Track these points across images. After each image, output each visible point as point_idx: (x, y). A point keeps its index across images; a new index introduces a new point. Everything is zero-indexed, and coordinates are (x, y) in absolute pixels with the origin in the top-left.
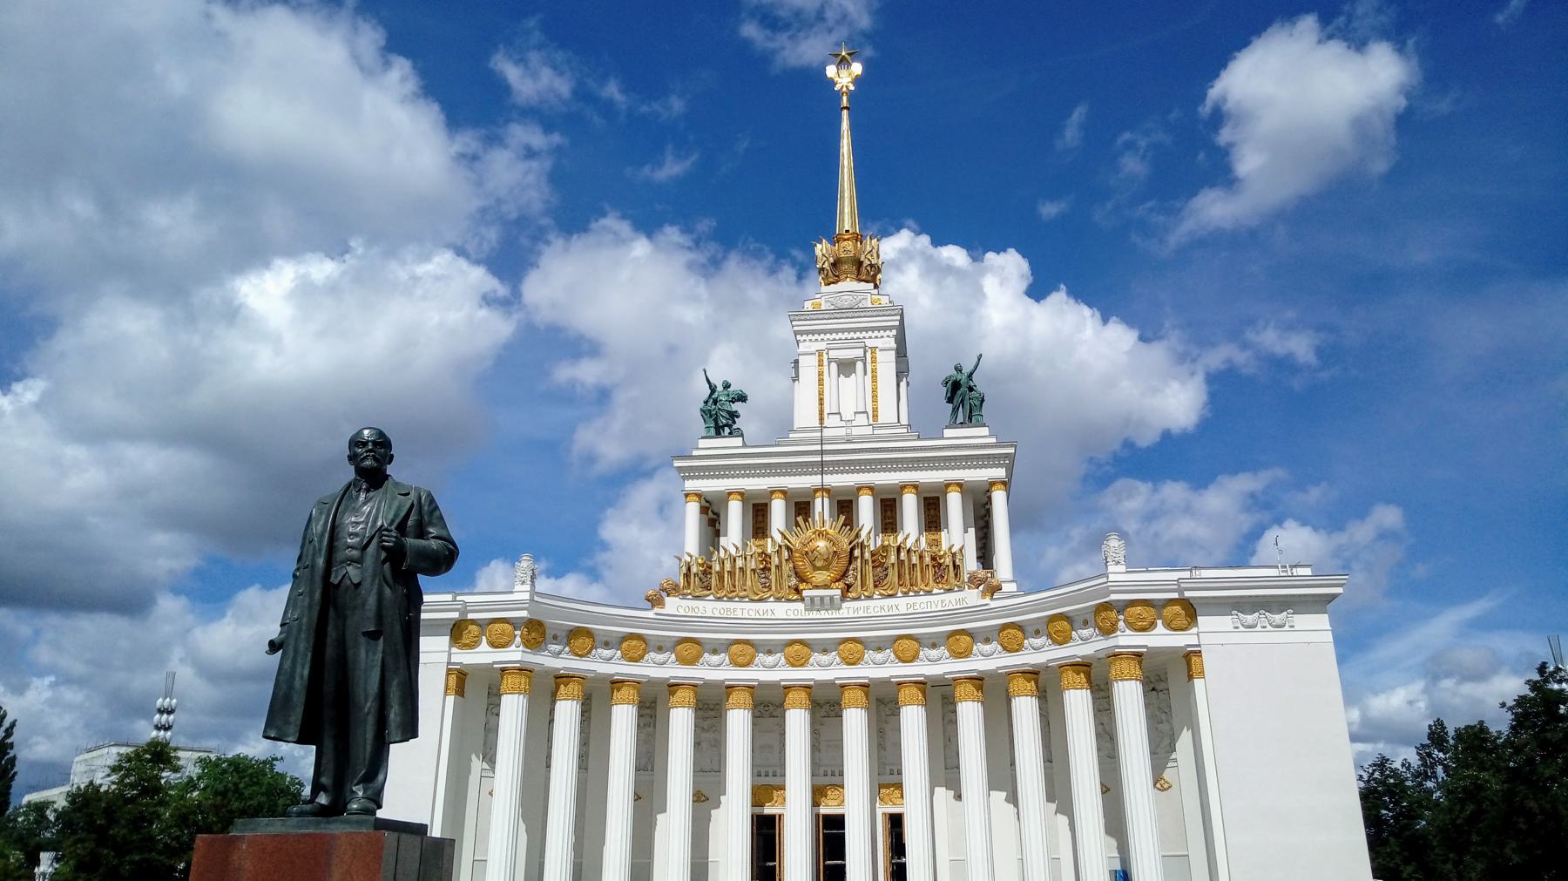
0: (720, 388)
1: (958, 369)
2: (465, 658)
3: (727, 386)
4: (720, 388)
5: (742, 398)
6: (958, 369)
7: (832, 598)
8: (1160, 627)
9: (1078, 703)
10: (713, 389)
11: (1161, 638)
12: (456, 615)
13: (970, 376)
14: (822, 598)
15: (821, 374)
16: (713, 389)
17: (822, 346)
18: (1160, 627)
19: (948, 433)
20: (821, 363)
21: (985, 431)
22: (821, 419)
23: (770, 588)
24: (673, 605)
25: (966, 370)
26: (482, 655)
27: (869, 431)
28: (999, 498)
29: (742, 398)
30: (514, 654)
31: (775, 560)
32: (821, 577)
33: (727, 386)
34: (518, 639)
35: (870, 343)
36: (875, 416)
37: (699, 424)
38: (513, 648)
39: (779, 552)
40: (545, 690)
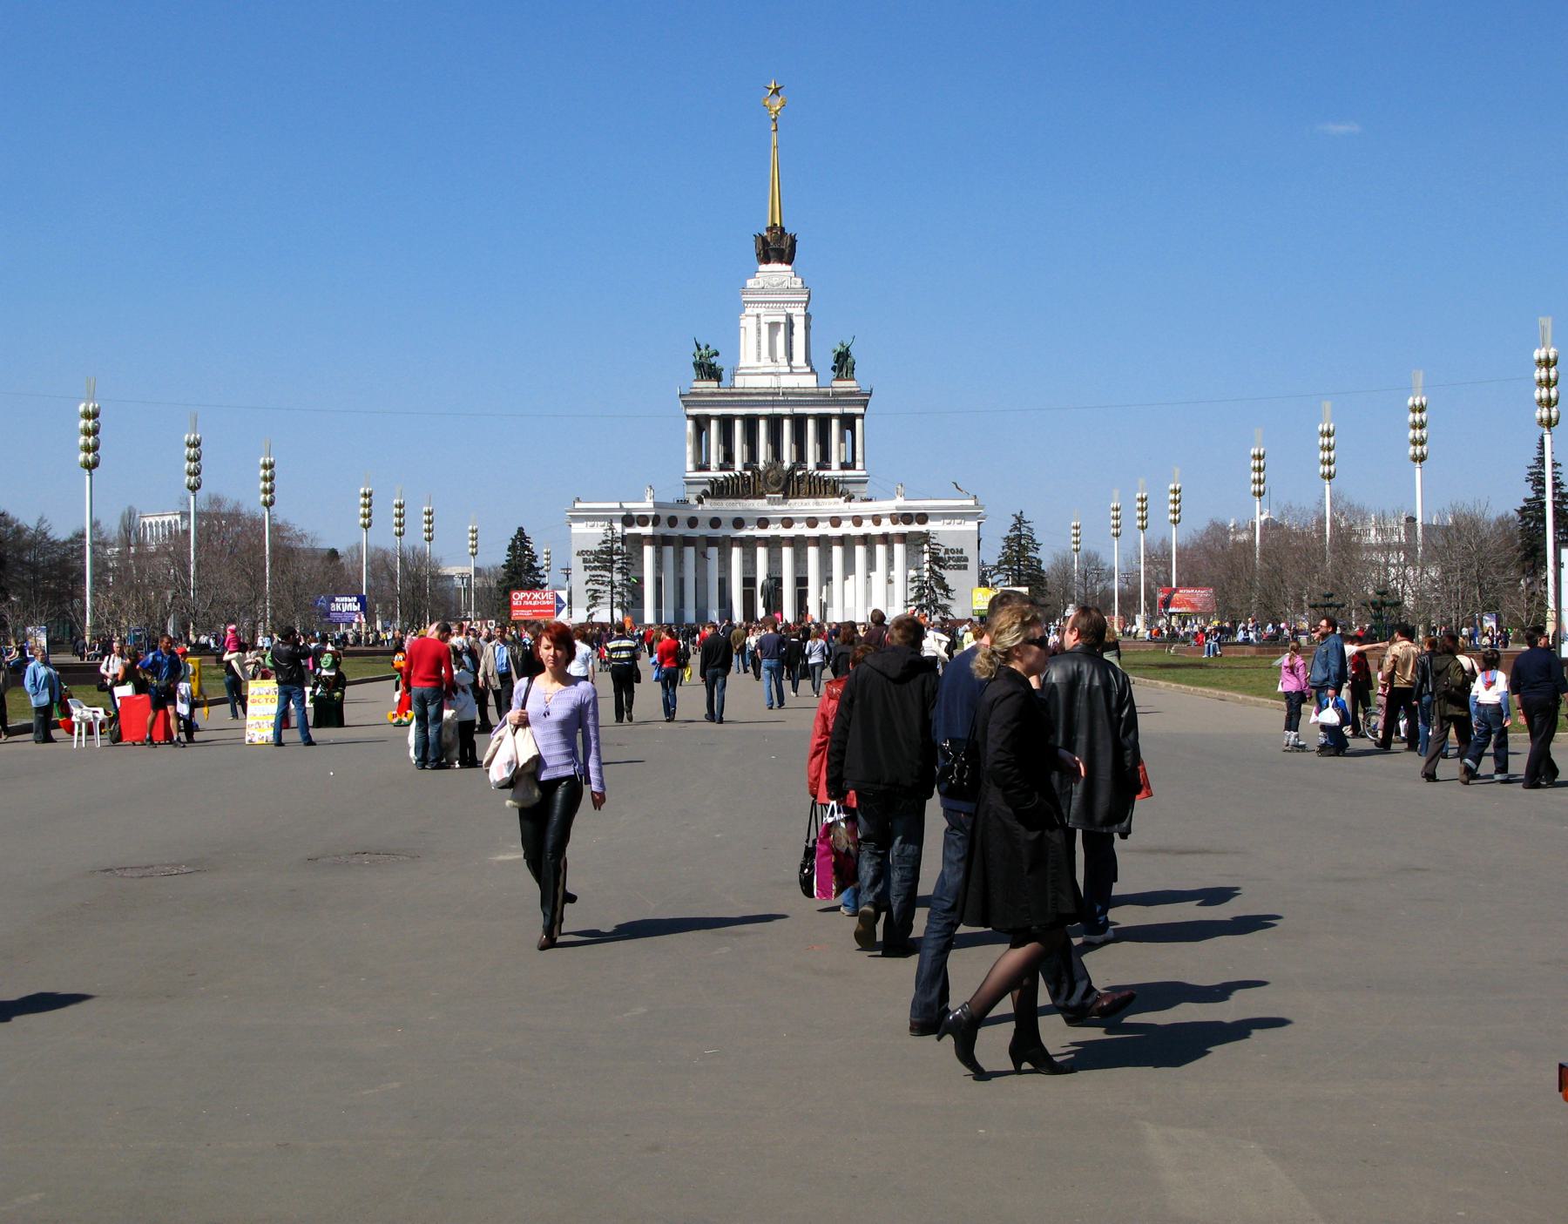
2: (629, 531)
5: (717, 354)
9: (881, 550)
15: (759, 330)
19: (836, 384)
20: (759, 323)
21: (853, 383)
22: (759, 359)
24: (708, 504)
26: (637, 530)
28: (858, 422)
30: (648, 530)
35: (789, 311)
36: (790, 357)
37: (693, 372)
40: (659, 542)
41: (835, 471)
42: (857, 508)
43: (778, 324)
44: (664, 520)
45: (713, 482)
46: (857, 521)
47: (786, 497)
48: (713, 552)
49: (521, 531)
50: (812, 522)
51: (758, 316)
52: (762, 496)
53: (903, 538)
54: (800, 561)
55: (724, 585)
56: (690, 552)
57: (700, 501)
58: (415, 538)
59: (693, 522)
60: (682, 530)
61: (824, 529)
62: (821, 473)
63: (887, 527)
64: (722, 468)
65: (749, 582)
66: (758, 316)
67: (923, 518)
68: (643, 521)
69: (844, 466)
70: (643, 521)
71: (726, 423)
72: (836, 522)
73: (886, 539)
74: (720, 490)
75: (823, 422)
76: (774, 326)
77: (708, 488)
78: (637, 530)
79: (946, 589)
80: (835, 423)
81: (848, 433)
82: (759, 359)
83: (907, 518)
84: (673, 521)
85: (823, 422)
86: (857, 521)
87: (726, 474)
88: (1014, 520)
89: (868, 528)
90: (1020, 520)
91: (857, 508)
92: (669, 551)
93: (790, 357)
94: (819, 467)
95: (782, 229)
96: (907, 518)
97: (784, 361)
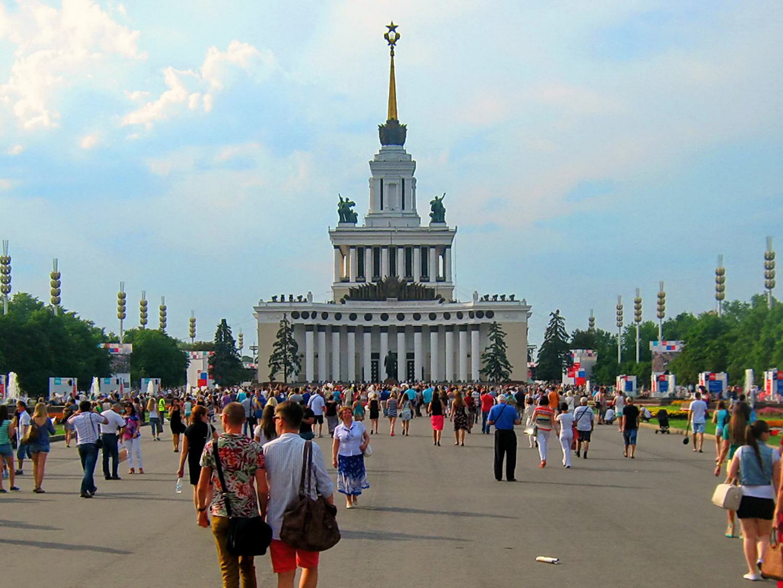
0: (344, 200)
1: (436, 198)
3: (347, 199)
4: (344, 200)
5: (354, 205)
6: (436, 198)
7: (395, 300)
8: (485, 317)
10: (341, 199)
11: (485, 320)
12: (293, 310)
13: (441, 200)
14: (392, 300)
16: (341, 199)
17: (382, 176)
18: (485, 317)
22: (382, 209)
23: (376, 297)
25: (439, 198)
27: (400, 215)
29: (354, 205)
30: (309, 321)
31: (377, 288)
32: (392, 294)
33: (347, 199)
34: (310, 317)
35: (403, 176)
36: (403, 208)
38: (308, 319)
39: (379, 286)
41: (431, 284)
42: (447, 306)
43: (395, 185)
44: (319, 316)
45: (352, 290)
46: (447, 316)
47: (399, 300)
48: (352, 335)
49: (224, 321)
50: (417, 317)
51: (382, 180)
52: (384, 300)
53: (476, 327)
54: (409, 341)
55: (358, 357)
56: (336, 335)
57: (343, 302)
58: (154, 325)
59: (338, 316)
60: (331, 321)
61: (425, 321)
62: (423, 284)
63: (467, 320)
64: (357, 281)
65: (375, 356)
66: (382, 180)
67: (490, 314)
68: (305, 315)
69: (438, 280)
70: (305, 315)
71: (361, 251)
72: (433, 317)
73: (464, 328)
74: (356, 295)
75: (424, 250)
76: (392, 186)
77: (348, 294)
78: (301, 321)
79: (507, 363)
80: (432, 250)
81: (441, 257)
82: (382, 209)
83: (480, 314)
84: (325, 316)
85: (424, 250)
86: (447, 316)
87: (360, 284)
88: (552, 317)
89: (454, 321)
90: (556, 317)
91: (447, 306)
92: (322, 335)
93: (403, 208)
94: (421, 281)
95: (398, 122)
96: (480, 314)
97: (399, 210)
